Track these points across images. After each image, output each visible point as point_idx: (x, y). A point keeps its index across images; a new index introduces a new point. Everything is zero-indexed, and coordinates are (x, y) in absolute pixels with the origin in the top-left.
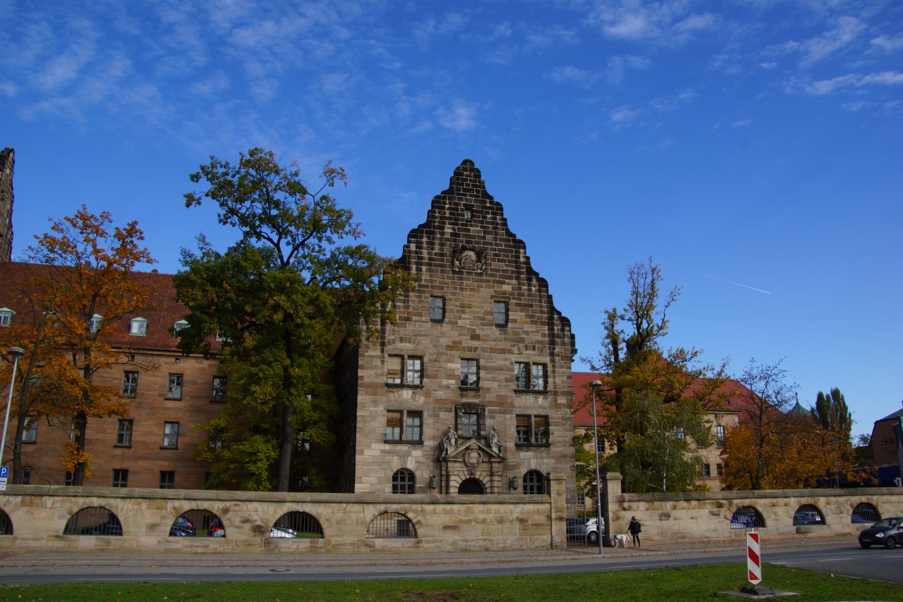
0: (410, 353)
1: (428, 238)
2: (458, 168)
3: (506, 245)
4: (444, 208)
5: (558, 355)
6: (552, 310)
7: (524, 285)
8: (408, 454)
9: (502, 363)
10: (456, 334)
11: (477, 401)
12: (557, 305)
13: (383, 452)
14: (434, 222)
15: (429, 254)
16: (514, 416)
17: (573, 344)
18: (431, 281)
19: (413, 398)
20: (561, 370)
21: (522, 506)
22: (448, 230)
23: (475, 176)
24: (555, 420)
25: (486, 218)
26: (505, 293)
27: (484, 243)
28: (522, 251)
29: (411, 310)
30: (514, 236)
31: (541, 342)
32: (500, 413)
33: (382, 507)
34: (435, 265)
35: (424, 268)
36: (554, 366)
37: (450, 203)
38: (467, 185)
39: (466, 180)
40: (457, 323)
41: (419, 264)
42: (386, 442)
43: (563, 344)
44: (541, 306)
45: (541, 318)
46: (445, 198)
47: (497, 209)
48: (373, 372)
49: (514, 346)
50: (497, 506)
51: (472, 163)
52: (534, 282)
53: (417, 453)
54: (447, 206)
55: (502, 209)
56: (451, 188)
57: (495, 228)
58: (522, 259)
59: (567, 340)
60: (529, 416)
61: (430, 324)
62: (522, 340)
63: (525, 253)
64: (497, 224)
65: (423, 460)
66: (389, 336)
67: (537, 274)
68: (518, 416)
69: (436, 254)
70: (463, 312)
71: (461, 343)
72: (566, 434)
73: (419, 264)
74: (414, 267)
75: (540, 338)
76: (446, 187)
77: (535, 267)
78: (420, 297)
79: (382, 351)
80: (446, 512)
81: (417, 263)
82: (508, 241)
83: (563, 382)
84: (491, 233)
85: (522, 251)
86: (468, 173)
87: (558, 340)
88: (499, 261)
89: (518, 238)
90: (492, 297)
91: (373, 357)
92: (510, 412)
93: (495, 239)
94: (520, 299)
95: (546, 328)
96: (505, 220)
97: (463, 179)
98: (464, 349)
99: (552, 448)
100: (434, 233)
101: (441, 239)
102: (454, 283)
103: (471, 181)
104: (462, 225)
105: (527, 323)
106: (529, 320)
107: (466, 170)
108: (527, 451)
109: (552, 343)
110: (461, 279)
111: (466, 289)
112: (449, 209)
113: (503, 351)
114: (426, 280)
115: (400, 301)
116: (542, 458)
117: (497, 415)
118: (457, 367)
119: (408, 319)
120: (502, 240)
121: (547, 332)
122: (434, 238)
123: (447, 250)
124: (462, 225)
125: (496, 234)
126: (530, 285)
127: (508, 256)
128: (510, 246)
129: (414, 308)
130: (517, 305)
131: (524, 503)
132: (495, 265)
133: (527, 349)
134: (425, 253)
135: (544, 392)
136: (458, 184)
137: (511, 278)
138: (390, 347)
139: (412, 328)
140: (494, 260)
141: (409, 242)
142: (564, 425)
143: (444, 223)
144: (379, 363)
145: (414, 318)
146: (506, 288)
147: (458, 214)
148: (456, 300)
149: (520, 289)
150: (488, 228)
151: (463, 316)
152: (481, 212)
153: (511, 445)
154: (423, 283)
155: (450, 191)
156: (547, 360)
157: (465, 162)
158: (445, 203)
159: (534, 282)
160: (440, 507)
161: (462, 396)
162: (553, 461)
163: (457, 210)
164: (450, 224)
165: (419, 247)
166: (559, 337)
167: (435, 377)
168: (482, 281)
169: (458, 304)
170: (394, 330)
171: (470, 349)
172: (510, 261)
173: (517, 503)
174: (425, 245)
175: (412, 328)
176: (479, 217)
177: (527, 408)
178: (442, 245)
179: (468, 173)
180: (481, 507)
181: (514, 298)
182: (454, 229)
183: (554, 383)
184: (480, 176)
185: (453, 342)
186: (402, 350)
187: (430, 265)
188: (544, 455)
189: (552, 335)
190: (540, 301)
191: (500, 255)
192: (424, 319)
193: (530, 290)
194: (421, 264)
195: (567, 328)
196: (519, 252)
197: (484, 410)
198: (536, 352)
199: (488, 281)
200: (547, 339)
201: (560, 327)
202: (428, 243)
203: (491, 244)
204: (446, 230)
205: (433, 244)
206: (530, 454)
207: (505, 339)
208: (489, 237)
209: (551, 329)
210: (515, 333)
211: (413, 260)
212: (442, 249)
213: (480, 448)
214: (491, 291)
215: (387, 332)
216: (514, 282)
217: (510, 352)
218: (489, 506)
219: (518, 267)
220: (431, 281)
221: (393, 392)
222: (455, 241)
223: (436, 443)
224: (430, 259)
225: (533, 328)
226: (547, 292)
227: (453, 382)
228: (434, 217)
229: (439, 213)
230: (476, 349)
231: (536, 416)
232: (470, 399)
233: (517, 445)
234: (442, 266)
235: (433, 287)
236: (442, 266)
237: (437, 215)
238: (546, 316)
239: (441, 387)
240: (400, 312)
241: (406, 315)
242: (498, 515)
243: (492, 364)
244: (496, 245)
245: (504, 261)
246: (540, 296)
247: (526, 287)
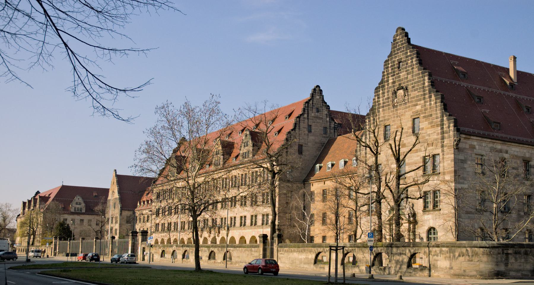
1: (382, 90)
2: (394, 37)
5: (446, 146)
9: (416, 159)
15: (383, 100)
22: (391, 81)
31: (436, 139)
35: (381, 110)
36: (443, 154)
39: (398, 42)
54: (390, 65)
56: (391, 52)
57: (413, 68)
58: (426, 84)
73: (379, 108)
75: (436, 137)
83: (449, 165)
90: (411, 116)
93: (413, 76)
94: (425, 113)
95: (439, 128)
99: (441, 212)
100: (383, 86)
103: (400, 42)
106: (430, 126)
107: (397, 35)
108: (428, 214)
109: (443, 138)
110: (397, 110)
112: (392, 66)
120: (416, 75)
122: (384, 89)
123: (390, 95)
127: (418, 85)
128: (420, 78)
130: (424, 117)
136: (394, 47)
137: (420, 100)
140: (412, 91)
141: (375, 96)
143: (388, 77)
146: (418, 108)
148: (395, 124)
149: (425, 105)
150: (409, 70)
154: (381, 119)
155: (390, 55)
165: (379, 98)
166: (447, 133)
168: (406, 108)
172: (420, 88)
178: (388, 92)
181: (422, 113)
182: (393, 79)
183: (444, 166)
189: (443, 133)
190: (436, 110)
193: (430, 104)
196: (424, 80)
198: (434, 147)
199: (409, 107)
200: (440, 136)
201: (447, 125)
203: (410, 81)
208: (410, 76)
209: (442, 128)
212: (388, 95)
219: (424, 91)
220: (384, 117)
224: (384, 103)
236: (389, 105)
238: (439, 119)
244: (413, 80)
245: (417, 89)
246: (436, 107)
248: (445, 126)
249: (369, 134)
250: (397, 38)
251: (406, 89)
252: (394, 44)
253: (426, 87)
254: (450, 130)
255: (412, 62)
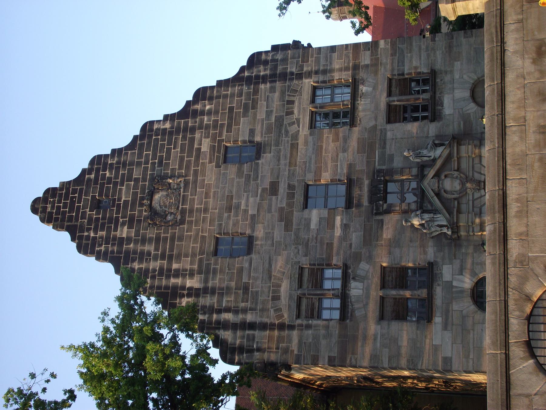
0: (296, 285)
1: (133, 260)
2: (42, 220)
3: (148, 149)
4: (94, 238)
5: (302, 67)
6: (238, 79)
7: (202, 121)
8: (449, 286)
10: (268, 216)
11: (366, 182)
12: (230, 72)
13: (445, 327)
14: (112, 252)
15: (155, 259)
16: (389, 126)
17: (285, 47)
18: (194, 255)
19: (362, 279)
20: (322, 62)
21: (509, 54)
22: (124, 232)
23: (54, 196)
24: (396, 65)
25: (110, 178)
26: (212, 148)
27: (144, 180)
28: (156, 126)
29: (233, 284)
30: (135, 137)
31: (283, 93)
32: (384, 148)
33: (517, 351)
34: (171, 249)
35: (175, 266)
37: (89, 230)
38: (65, 206)
40: (253, 216)
41: (169, 273)
42: (429, 320)
43: (285, 60)
44: (233, 95)
45: (248, 94)
46: (81, 238)
47: (99, 163)
48: (323, 342)
49: (287, 132)
50: (510, 107)
51: (36, 201)
52: (198, 107)
53: (447, 272)
55: (100, 157)
58: (168, 125)
59: (279, 56)
60: (390, 108)
61: (253, 256)
62: (280, 120)
63: (158, 121)
64: (118, 163)
65: (457, 263)
66: (271, 318)
67: (188, 103)
68: (389, 121)
69: (156, 249)
70: (238, 206)
71: (281, 209)
72: (415, 49)
73: (169, 273)
74: (173, 281)
75: (277, 95)
76: (65, 235)
77: (177, 107)
78: (215, 271)
79: (291, 327)
80: (523, 213)
81: (168, 277)
82: (142, 145)
84: (131, 172)
85: (156, 126)
86: (49, 206)
87: (280, 68)
88: (168, 158)
89: (138, 133)
91: (300, 342)
92: (383, 132)
93: (139, 164)
94: (222, 125)
95: (262, 86)
96: (114, 151)
97: (57, 213)
98: (290, 205)
99: (438, 66)
100: (127, 253)
101: (136, 242)
102: (197, 222)
103: (59, 202)
104: (118, 212)
105: (255, 115)
108: (442, 105)
109: (284, 76)
110: (191, 211)
111: (206, 203)
112: (96, 232)
113: (294, 146)
114: (192, 263)
115: (220, 301)
116: (453, 81)
117: (388, 152)
118: (315, 215)
119: (246, 289)
120: (140, 156)
121: (268, 85)
122: (135, 252)
123: (151, 233)
124: (118, 212)
125: (131, 164)
126: (202, 113)
127: (163, 146)
128: (149, 144)
129: (231, 280)
130: (229, 130)
131: (503, 51)
132: (174, 164)
133: (292, 113)
134: (154, 265)
135: (354, 85)
137: (192, 140)
138: (286, 316)
139: (259, 282)
142: (403, 51)
144: (310, 332)
145: (245, 280)
147: (104, 218)
148: (220, 218)
149: (207, 127)
150: (123, 175)
151: (243, 207)
152: (102, 185)
153: (432, 128)
154: (196, 267)
156: (308, 83)
157: (34, 210)
158: (88, 237)
159: (198, 107)
160: (515, 226)
161: (359, 205)
162: (457, 64)
163: (97, 219)
164: (116, 230)
166: (275, 67)
167: (330, 245)
168: (195, 182)
169: (226, 215)
170: (262, 310)
171: (291, 196)
172: (169, 143)
173: (503, 64)
174: (143, 266)
175: (259, 282)
176: (108, 189)
177: (377, 107)
178: (144, 241)
179: (49, 206)
180: (512, 138)
181: (221, 134)
182: (123, 224)
183: (340, 70)
184: (54, 189)
185: (281, 220)
186: (291, 297)
187: (171, 257)
188: (447, 78)
189: (273, 78)
190: (226, 96)
191: (161, 157)
192: (246, 265)
193: (209, 113)
194: (169, 270)
195: (263, 57)
196: (158, 129)
197: (379, 171)
198: (296, 99)
199: (196, 172)
200: (278, 85)
201: (262, 67)
202: (141, 262)
203: (146, 169)
204: (124, 235)
205: (142, 253)
206: (447, 100)
207: (277, 144)
209: (264, 79)
210: (269, 130)
211: (164, 282)
213: (437, 175)
214: (210, 167)
215: (265, 320)
216: (197, 135)
217: (295, 136)
218: (509, 123)
219: (178, 131)
221: (353, 311)
222: (139, 221)
223: (431, 243)
224: (163, 257)
225: (262, 105)
226: (212, 88)
227: (338, 219)
228: (106, 253)
229: (100, 245)
230: (291, 187)
231: (390, 94)
232: (363, 193)
233: (433, 120)
234: (173, 239)
235: (202, 253)
236: (173, 239)
237: (103, 248)
238: (245, 88)
239: (344, 237)
240: (236, 301)
241: (241, 292)
242: (529, 101)
243: (313, 161)
244: (147, 162)
245: (169, 150)
246: (218, 97)
247: (206, 118)
248: (262, 74)
249: (219, 311)
250: (49, 210)
251: (159, 181)
252: (57, 219)
253: (172, 127)
254: (273, 60)
255: (112, 164)
